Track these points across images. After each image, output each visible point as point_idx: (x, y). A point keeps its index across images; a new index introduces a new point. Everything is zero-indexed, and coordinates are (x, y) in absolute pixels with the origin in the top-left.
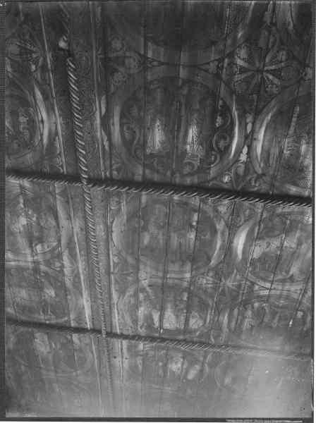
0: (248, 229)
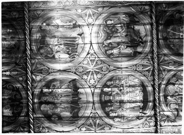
0: (49, 64)
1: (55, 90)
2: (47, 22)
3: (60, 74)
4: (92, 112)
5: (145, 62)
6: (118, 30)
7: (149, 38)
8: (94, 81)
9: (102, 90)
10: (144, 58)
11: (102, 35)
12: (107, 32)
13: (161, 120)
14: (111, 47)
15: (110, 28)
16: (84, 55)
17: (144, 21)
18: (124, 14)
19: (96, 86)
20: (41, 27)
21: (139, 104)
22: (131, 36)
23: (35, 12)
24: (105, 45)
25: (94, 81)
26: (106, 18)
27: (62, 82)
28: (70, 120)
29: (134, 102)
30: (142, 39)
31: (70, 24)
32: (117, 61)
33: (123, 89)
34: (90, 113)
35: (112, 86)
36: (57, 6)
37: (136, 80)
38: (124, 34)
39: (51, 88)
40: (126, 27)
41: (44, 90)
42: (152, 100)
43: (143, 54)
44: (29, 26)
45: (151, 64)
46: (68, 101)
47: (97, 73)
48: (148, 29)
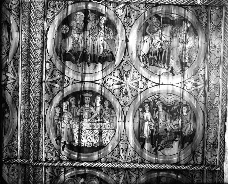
0: (137, 27)
1: (103, 32)
2: (192, 29)
3: (123, 41)
4: (71, 79)
5: (131, 153)
6: (175, 120)
7: (175, 159)
8: (111, 85)
9: (98, 94)
10: (135, 151)
11: (170, 100)
12: (172, 106)
13: (53, 168)
14: (153, 109)
15: (177, 110)
16: (146, 75)
17: (183, 155)
18: (193, 129)
19: (104, 87)
20: (185, 20)
21: (77, 141)
22: (166, 136)
23: (205, 14)
24: (156, 103)
25: (111, 85)
26: (190, 106)
27: (112, 42)
28: (61, 49)
29: (80, 134)
30: (160, 150)
31: (187, 58)
32: (135, 116)
33: (98, 122)
34: (69, 76)
35: (102, 107)
36: (211, 43)
37: (108, 139)
38: (168, 128)
39: (106, 27)
40: (177, 131)
41: (104, 17)
42: (80, 158)
43: (141, 151)
44: (188, 5)
45: (128, 159)
46: (86, 48)
47: (121, 89)
48: (172, 159)
